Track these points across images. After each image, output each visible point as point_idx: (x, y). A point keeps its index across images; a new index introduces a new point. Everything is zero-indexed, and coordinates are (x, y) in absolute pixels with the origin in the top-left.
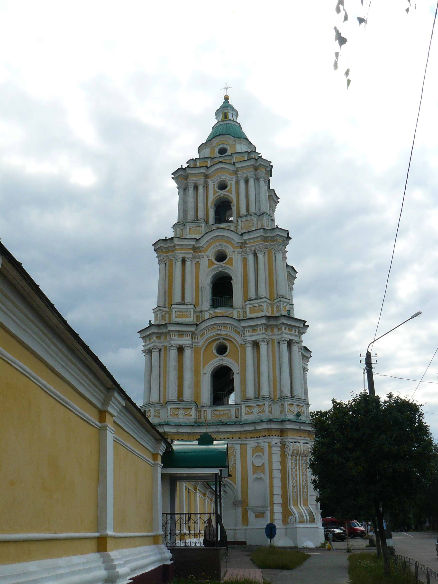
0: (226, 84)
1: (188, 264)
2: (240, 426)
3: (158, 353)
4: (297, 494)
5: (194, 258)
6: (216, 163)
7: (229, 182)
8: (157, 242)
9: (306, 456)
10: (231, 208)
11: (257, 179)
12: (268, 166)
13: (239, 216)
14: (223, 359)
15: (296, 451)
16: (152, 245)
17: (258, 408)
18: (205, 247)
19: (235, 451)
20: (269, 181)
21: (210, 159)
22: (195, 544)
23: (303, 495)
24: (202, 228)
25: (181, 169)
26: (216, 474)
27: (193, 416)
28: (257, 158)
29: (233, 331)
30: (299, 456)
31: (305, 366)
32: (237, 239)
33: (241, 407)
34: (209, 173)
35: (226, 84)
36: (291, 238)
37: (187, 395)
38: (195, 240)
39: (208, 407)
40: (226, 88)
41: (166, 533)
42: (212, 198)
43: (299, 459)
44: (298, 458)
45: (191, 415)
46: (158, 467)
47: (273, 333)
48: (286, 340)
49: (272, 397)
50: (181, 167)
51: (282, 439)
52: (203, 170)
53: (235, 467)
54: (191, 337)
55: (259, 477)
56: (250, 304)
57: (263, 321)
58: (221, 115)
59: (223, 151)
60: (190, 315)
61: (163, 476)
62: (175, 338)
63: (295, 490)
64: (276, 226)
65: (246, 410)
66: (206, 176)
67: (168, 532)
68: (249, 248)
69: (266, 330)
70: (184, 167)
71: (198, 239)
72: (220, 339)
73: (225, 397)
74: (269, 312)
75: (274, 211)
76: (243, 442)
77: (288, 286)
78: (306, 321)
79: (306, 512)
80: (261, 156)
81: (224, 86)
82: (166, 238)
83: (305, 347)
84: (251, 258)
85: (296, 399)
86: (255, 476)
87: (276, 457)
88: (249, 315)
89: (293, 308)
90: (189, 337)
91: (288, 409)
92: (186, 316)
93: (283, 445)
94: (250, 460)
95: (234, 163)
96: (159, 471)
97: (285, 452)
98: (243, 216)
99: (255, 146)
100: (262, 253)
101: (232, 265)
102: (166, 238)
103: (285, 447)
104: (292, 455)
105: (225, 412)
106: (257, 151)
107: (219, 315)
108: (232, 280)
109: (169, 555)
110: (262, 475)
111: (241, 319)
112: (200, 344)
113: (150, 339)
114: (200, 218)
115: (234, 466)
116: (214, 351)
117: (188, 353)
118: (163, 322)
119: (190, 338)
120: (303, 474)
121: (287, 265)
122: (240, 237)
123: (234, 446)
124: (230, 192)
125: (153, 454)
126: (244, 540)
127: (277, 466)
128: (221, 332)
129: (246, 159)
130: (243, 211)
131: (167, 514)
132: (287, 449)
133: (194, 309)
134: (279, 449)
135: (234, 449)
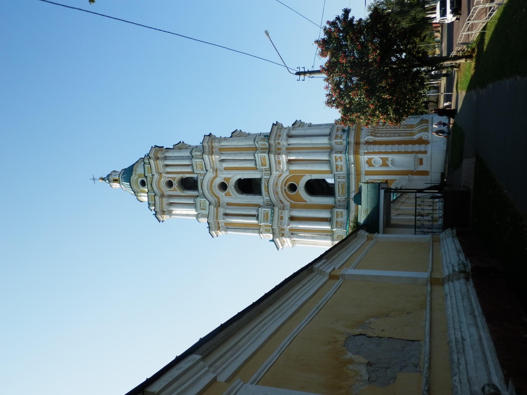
0: (91, 179)
1: (229, 211)
3: (293, 235)
4: (405, 133)
5: (223, 207)
6: (152, 188)
7: (168, 179)
8: (211, 234)
10: (188, 178)
11: (165, 158)
12: (155, 149)
13: (193, 173)
16: (213, 238)
17: (338, 161)
18: (215, 198)
20: (167, 149)
21: (148, 193)
22: (440, 209)
24: (201, 200)
25: (155, 215)
26: (385, 192)
28: (149, 157)
29: (279, 179)
30: (376, 131)
31: (307, 125)
32: (210, 175)
33: (336, 174)
34: (159, 194)
35: (91, 179)
36: (210, 133)
37: (325, 214)
38: (210, 206)
39: (336, 199)
40: (94, 179)
41: (431, 232)
42: (179, 192)
45: (342, 212)
46: (378, 236)
47: (282, 149)
48: (287, 139)
49: (329, 150)
50: (154, 215)
52: (157, 198)
53: (382, 180)
54: (282, 211)
55: (391, 162)
56: (259, 165)
57: (272, 156)
58: (114, 183)
59: (143, 183)
60: (266, 211)
61: (384, 233)
62: (283, 222)
64: (201, 144)
65: (339, 170)
66: (162, 196)
67: (430, 230)
68: (218, 165)
69: (279, 154)
70: (155, 213)
71: (209, 203)
72: (285, 189)
73: (329, 186)
74: (266, 151)
75: (190, 146)
77: (246, 136)
78: (273, 124)
79: (419, 126)
80: (147, 154)
81: (92, 180)
82: (208, 228)
83: (293, 125)
84: (225, 165)
85: (332, 132)
87: (377, 148)
88: (268, 167)
89: (263, 133)
90: (282, 212)
92: (267, 214)
93: (368, 143)
94: (377, 168)
95: (152, 175)
96: (381, 235)
98: (193, 170)
99: (140, 159)
101: (230, 179)
102: (208, 228)
103: (368, 141)
105: (340, 186)
106: (143, 157)
107: (267, 189)
108: (241, 179)
109: (448, 231)
110: (390, 159)
111: (270, 173)
112: (289, 204)
113: (284, 241)
114: (194, 201)
117: (296, 213)
118: (271, 230)
119: (283, 211)
121: (231, 137)
122: (208, 171)
124: (174, 179)
125: (367, 240)
126: (440, 174)
127: (383, 148)
129: (149, 166)
130: (189, 169)
131: (415, 231)
132: (370, 140)
133: (262, 208)
134: (369, 146)
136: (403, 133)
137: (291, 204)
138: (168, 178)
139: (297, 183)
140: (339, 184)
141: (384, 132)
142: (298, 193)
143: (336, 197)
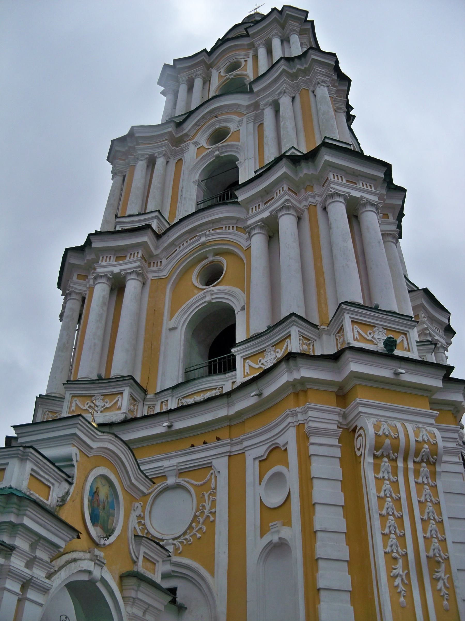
2: (225, 400)
7: (243, 61)
9: (428, 460)
14: (211, 291)
15: (387, 441)
17: (274, 351)
19: (216, 477)
23: (436, 591)
27: (124, 408)
30: (405, 460)
39: (170, 391)
43: (406, 470)
44: (400, 464)
47: (309, 193)
51: (344, 416)
53: (213, 521)
55: (275, 539)
63: (399, 569)
76: (235, 448)
86: (267, 538)
91: (356, 333)
97: (356, 450)
100: (285, 94)
104: (378, 453)
112: (165, 273)
115: (212, 519)
116: (196, 284)
120: (425, 517)
123: (213, 464)
128: (208, 238)
135: (212, 471)
136: (408, 575)
137: (167, 279)
138: (246, 61)
139: (223, 277)
140: (216, 388)
141: (403, 495)
142: (196, 291)
143: (175, 391)
